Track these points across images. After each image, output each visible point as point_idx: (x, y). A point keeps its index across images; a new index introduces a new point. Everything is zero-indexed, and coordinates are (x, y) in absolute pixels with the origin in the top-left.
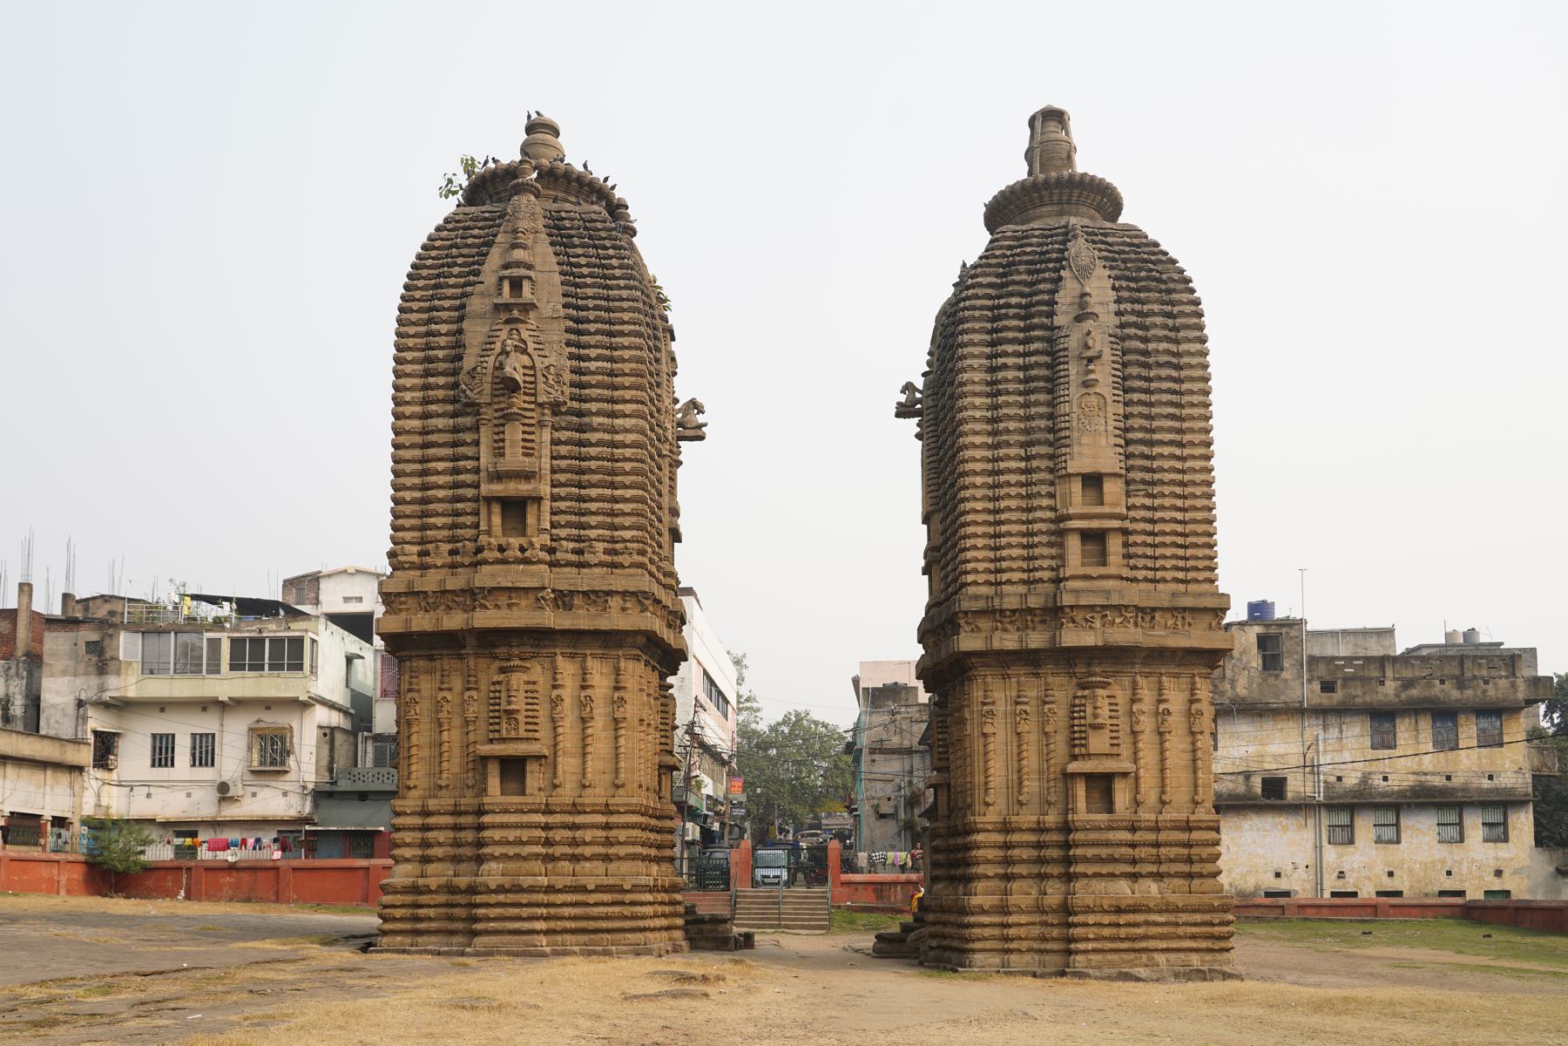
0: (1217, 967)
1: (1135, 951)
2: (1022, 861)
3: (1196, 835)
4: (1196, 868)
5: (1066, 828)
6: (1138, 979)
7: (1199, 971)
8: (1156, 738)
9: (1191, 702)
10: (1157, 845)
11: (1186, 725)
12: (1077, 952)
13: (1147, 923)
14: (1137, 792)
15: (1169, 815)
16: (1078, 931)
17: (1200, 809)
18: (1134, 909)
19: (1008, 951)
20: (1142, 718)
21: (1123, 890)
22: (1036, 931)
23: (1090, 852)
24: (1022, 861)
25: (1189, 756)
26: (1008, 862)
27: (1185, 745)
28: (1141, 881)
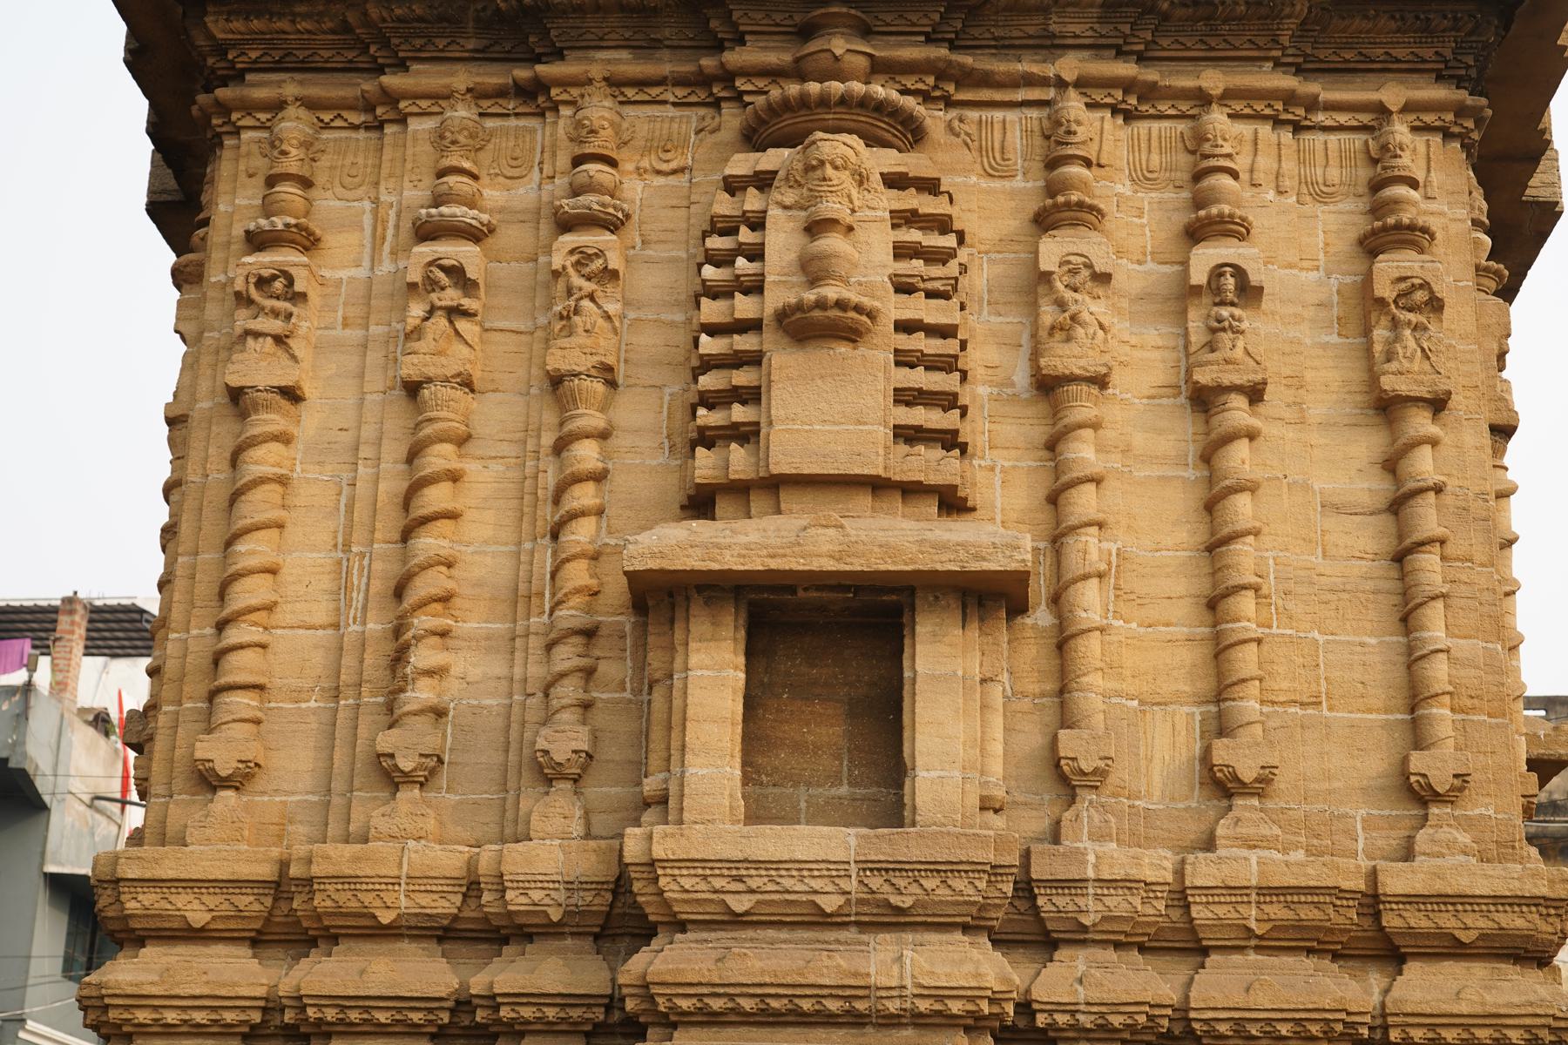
5: (621, 915)
8: (1177, 434)
9: (1372, 245)
11: (1357, 375)
14: (1066, 718)
17: (1444, 831)
20: (1092, 307)
25: (1364, 539)
27: (1344, 465)
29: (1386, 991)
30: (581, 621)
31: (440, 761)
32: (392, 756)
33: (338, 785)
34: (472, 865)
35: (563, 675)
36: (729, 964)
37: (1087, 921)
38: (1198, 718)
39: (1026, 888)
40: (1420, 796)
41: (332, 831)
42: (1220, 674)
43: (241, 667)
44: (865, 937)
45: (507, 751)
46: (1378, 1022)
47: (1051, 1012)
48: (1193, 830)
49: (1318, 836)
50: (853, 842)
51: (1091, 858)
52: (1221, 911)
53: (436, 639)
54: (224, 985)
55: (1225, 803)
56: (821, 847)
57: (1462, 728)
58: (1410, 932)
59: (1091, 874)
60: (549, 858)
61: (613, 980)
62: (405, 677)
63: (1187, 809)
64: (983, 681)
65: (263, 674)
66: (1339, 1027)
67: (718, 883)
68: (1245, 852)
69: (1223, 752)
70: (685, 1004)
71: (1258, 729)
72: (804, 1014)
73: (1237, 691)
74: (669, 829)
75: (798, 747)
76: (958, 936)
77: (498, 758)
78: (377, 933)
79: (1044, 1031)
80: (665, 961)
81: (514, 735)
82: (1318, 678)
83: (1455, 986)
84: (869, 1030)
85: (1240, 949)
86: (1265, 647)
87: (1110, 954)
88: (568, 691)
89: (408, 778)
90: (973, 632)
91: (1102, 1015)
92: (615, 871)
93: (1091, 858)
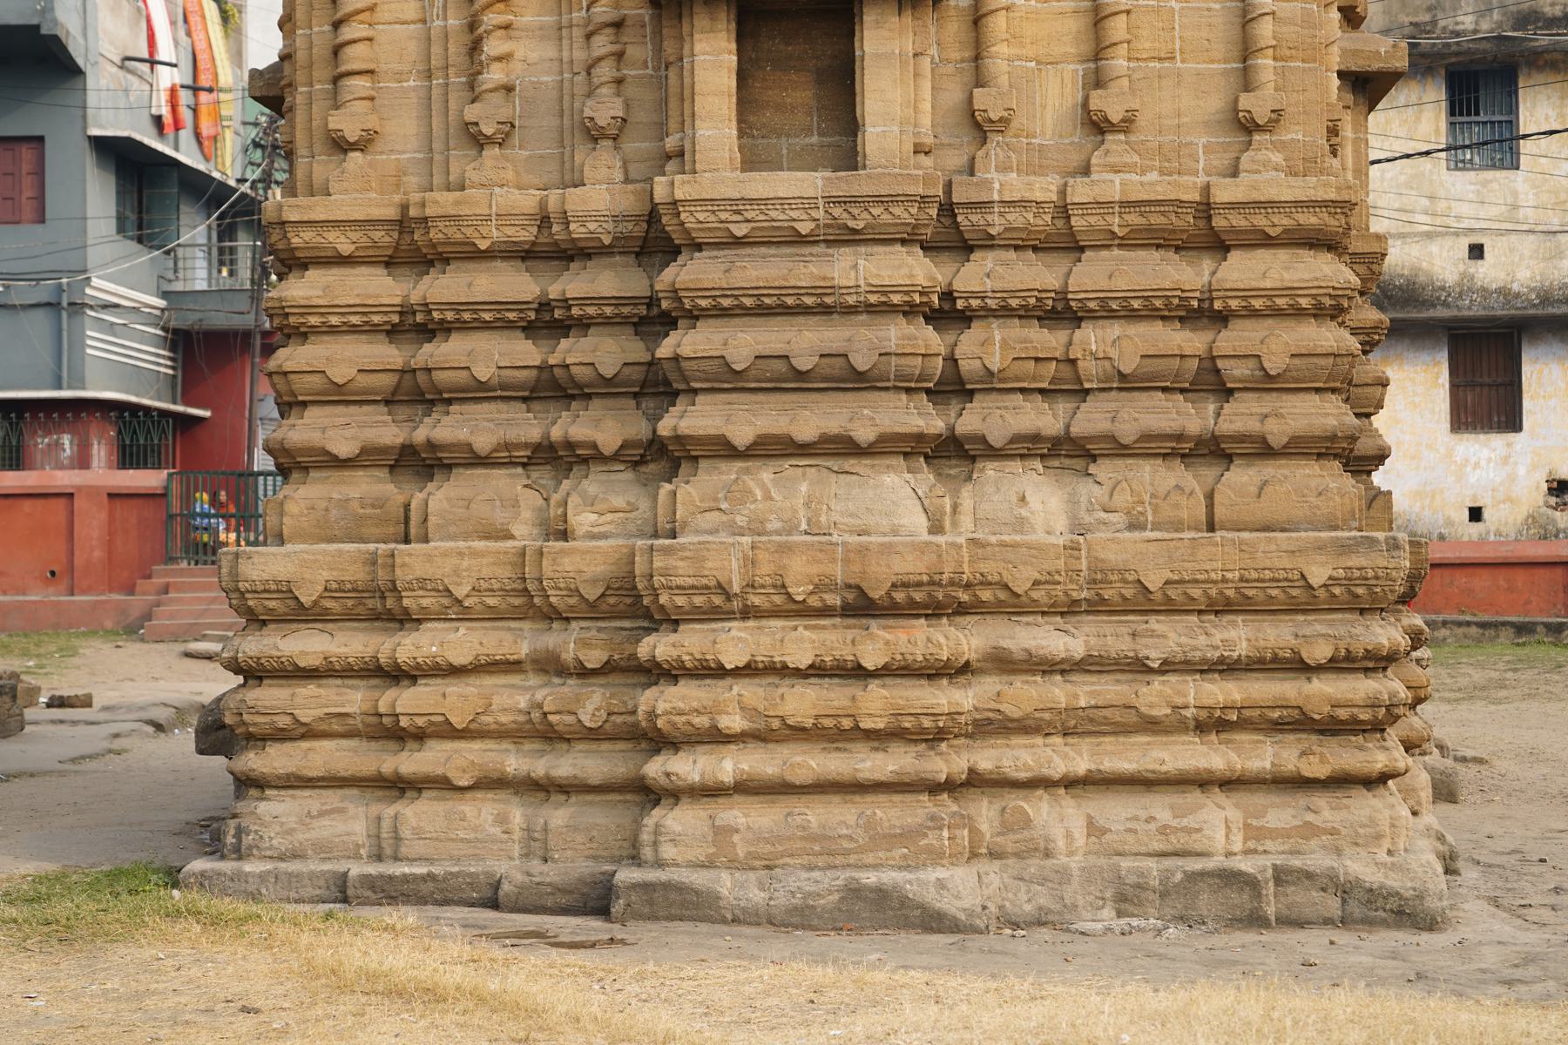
0: (1318, 860)
1: (934, 788)
2: (479, 392)
3: (1244, 271)
4: (1241, 416)
5: (654, 240)
6: (934, 922)
7: (1230, 878)
10: (1062, 312)
12: (672, 794)
13: (1003, 663)
15: (1121, 178)
16: (669, 703)
17: (1265, 153)
18: (936, 602)
19: (400, 786)
21: (890, 514)
22: (511, 698)
23: (742, 343)
24: (479, 392)
26: (416, 394)
28: (989, 471)
29: (1214, 273)
30: (612, 16)
31: (513, 126)
32: (477, 124)
33: (438, 145)
34: (543, 204)
35: (600, 59)
36: (734, 273)
37: (993, 232)
38: (1081, 73)
39: (948, 209)
40: (1247, 127)
41: (438, 180)
42: (1098, 39)
43: (355, 57)
44: (830, 251)
45: (562, 116)
46: (1206, 295)
47: (967, 298)
48: (1075, 159)
49: (1169, 160)
50: (820, 183)
51: (997, 186)
52: (1092, 220)
53: (502, 32)
54: (370, 297)
55: (1099, 138)
56: (799, 187)
57: (1281, 73)
58: (1233, 230)
59: (996, 197)
60: (599, 198)
61: (652, 286)
62: (481, 62)
63: (1072, 143)
64: (915, 55)
65: (372, 60)
66: (1176, 301)
67: (724, 216)
68: (1111, 176)
69: (1097, 101)
70: (703, 303)
71: (1125, 82)
72: (789, 307)
73: (1109, 52)
74: (685, 177)
75: (779, 108)
76: (898, 247)
77: (555, 122)
78: (474, 255)
79: (962, 311)
80: (688, 273)
81: (566, 105)
82: (1173, 39)
83: (1263, 269)
84: (835, 316)
85: (1107, 247)
86: (1133, 16)
87: (1012, 254)
88: (605, 71)
89: (490, 140)
90: (908, 18)
91: (1004, 299)
92: (648, 207)
93: (997, 186)
